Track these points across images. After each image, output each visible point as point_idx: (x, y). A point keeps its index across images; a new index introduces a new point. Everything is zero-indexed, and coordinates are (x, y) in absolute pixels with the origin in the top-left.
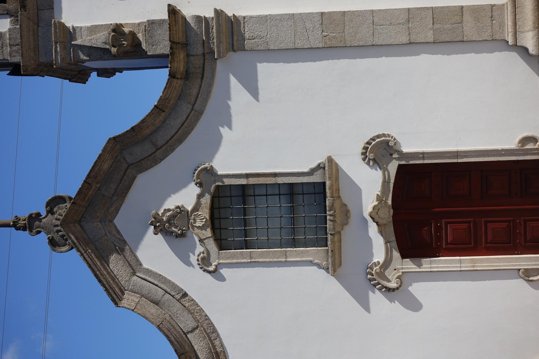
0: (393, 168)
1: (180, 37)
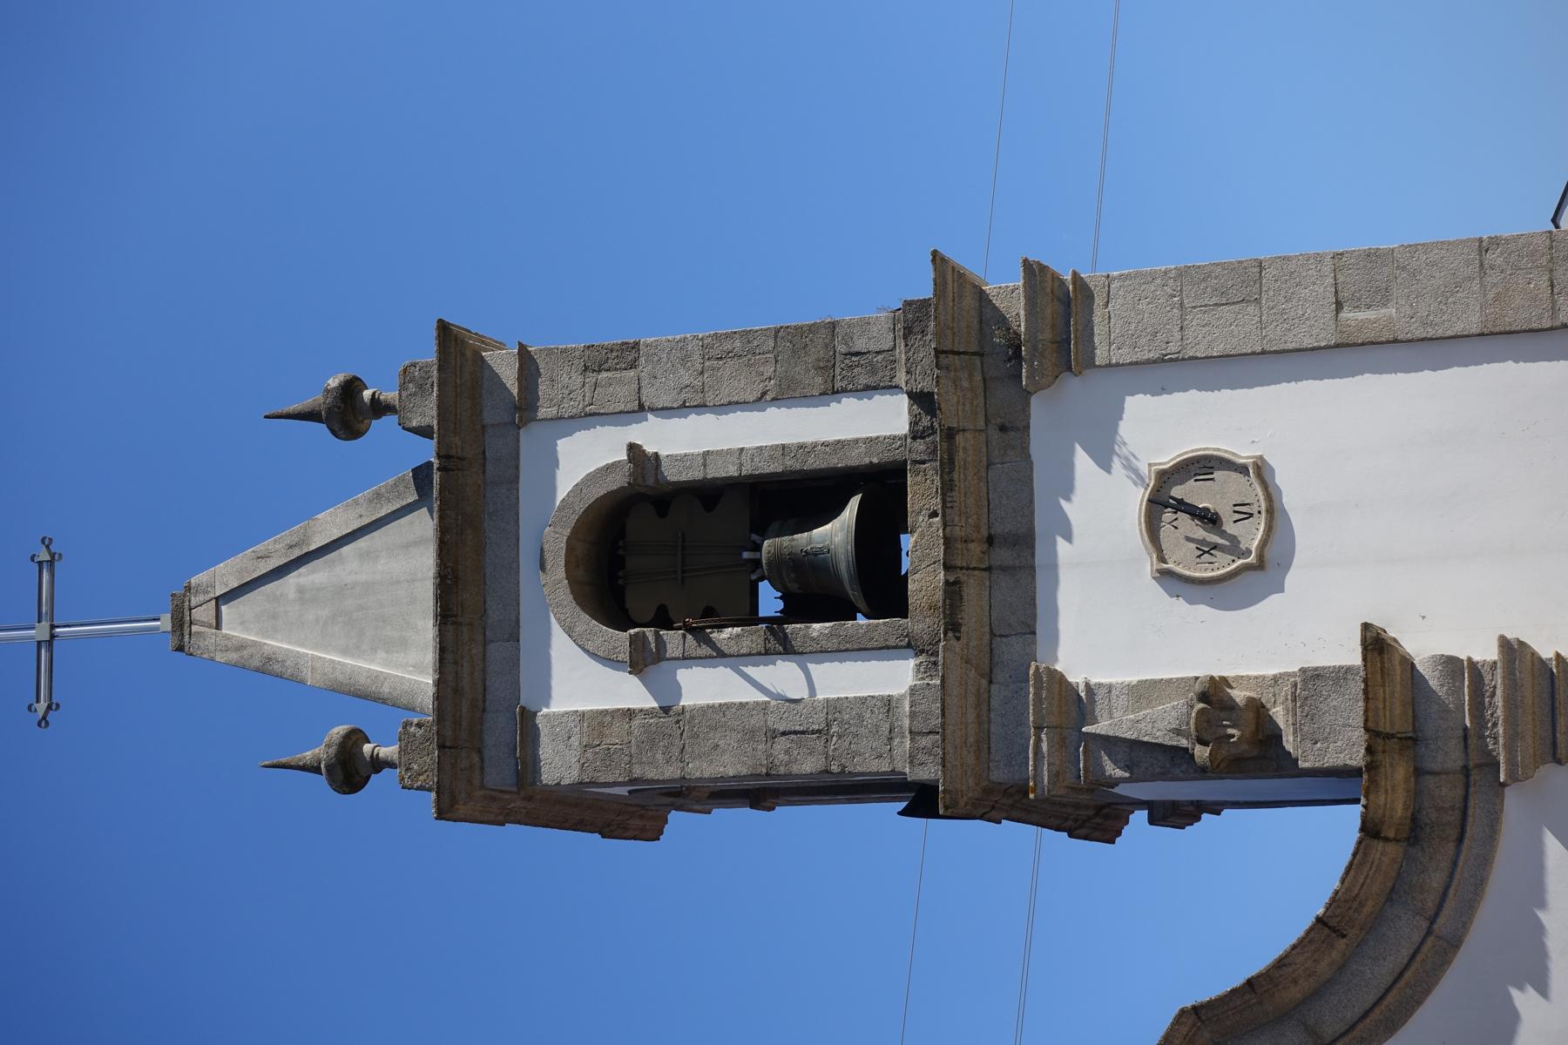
1: (1395, 720)
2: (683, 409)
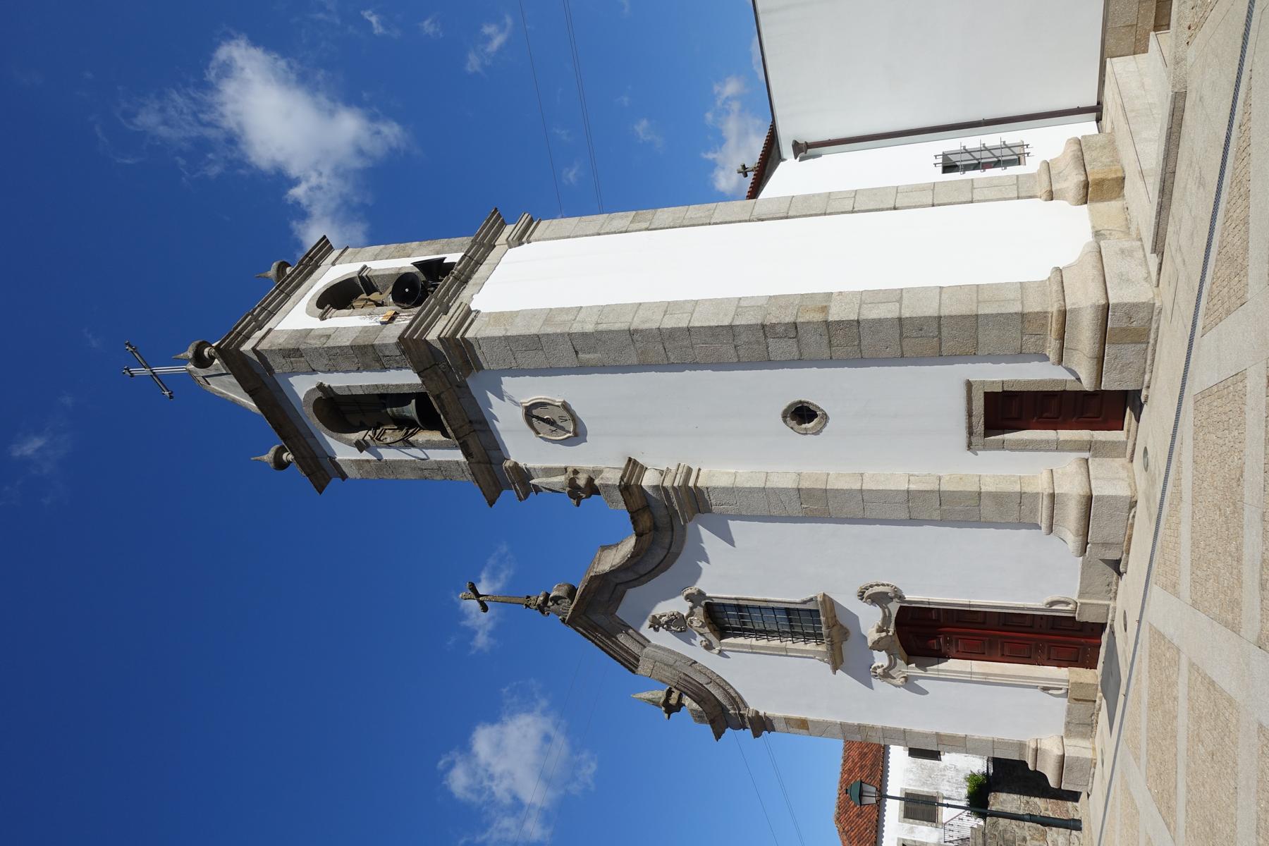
0: (894, 607)
1: (637, 503)
2: (329, 371)
